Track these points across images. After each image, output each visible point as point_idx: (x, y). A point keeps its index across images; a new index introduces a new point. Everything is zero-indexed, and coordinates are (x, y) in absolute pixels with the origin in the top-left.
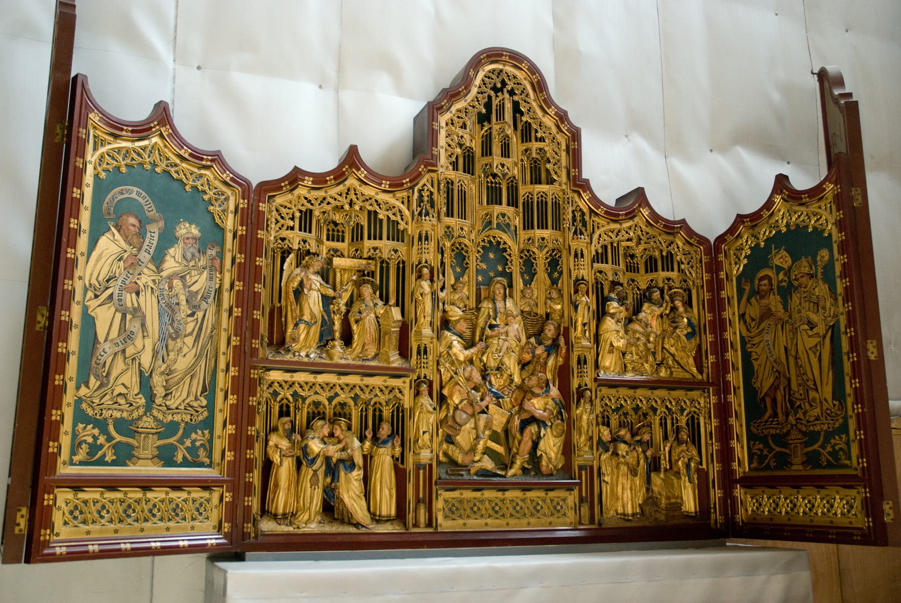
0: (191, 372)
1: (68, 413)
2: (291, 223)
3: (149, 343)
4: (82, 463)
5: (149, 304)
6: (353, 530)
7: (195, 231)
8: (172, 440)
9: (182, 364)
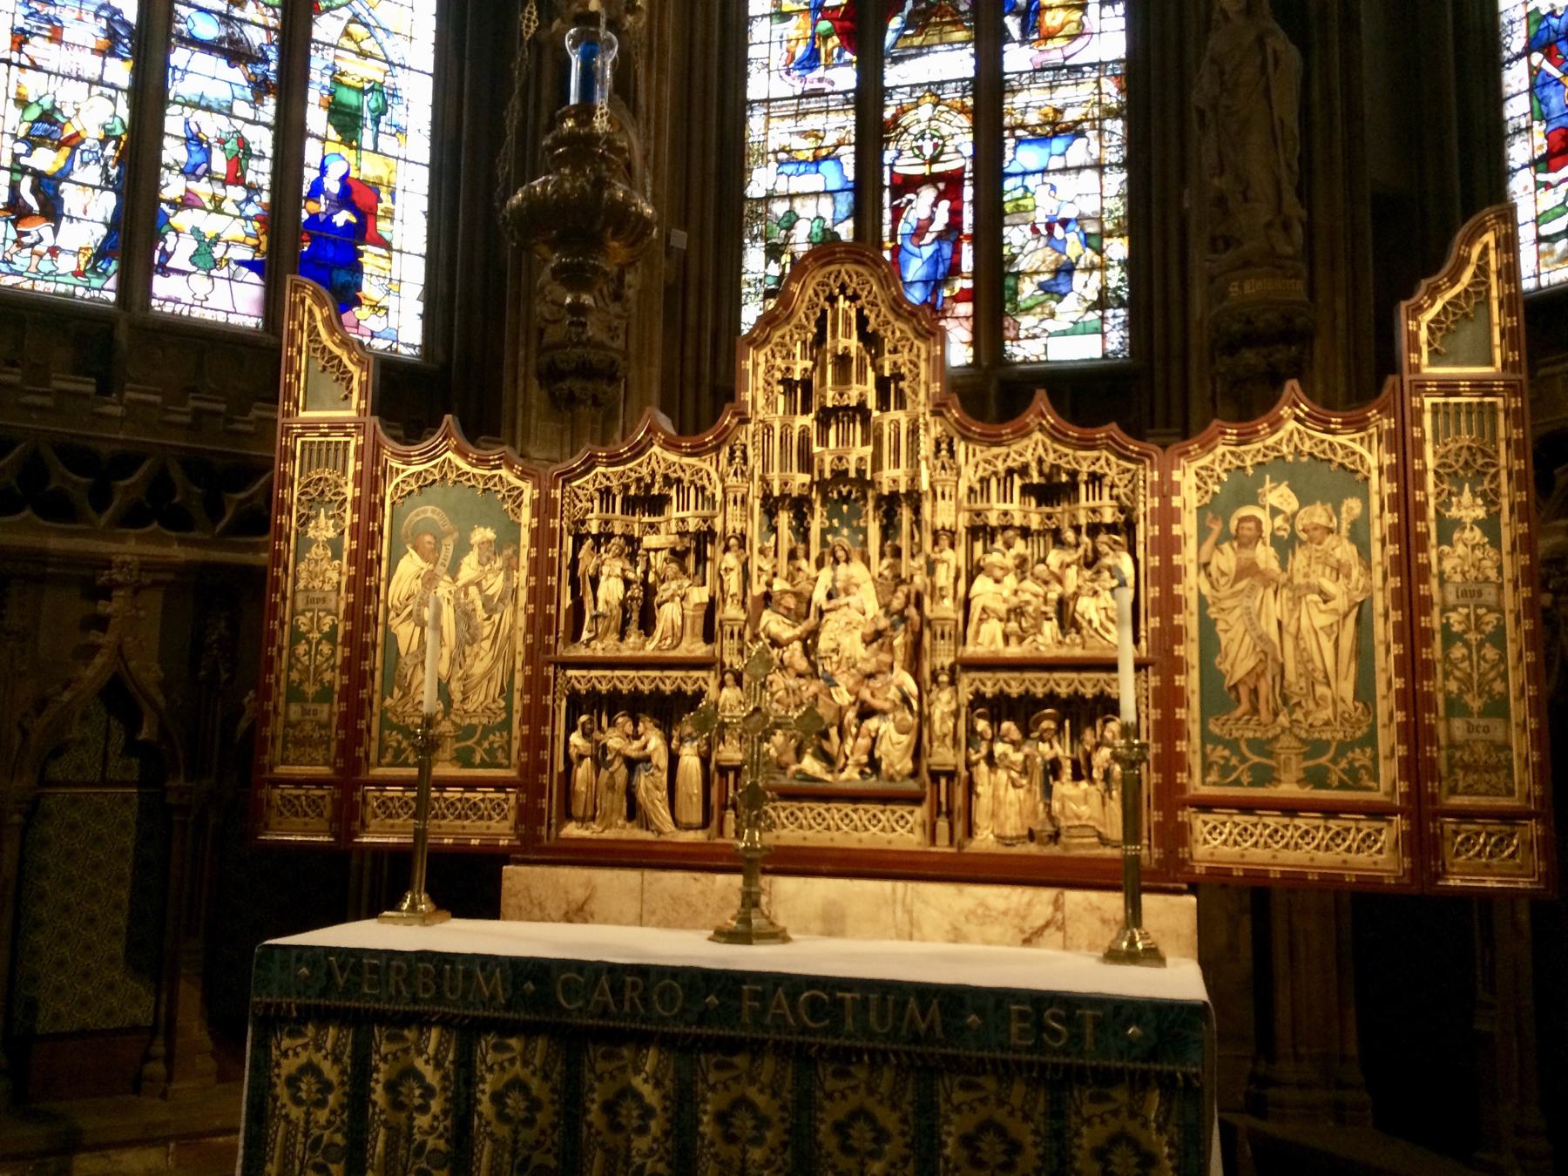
0: (488, 675)
2: (589, 505)
7: (490, 534)
8: (470, 743)
9: (479, 669)
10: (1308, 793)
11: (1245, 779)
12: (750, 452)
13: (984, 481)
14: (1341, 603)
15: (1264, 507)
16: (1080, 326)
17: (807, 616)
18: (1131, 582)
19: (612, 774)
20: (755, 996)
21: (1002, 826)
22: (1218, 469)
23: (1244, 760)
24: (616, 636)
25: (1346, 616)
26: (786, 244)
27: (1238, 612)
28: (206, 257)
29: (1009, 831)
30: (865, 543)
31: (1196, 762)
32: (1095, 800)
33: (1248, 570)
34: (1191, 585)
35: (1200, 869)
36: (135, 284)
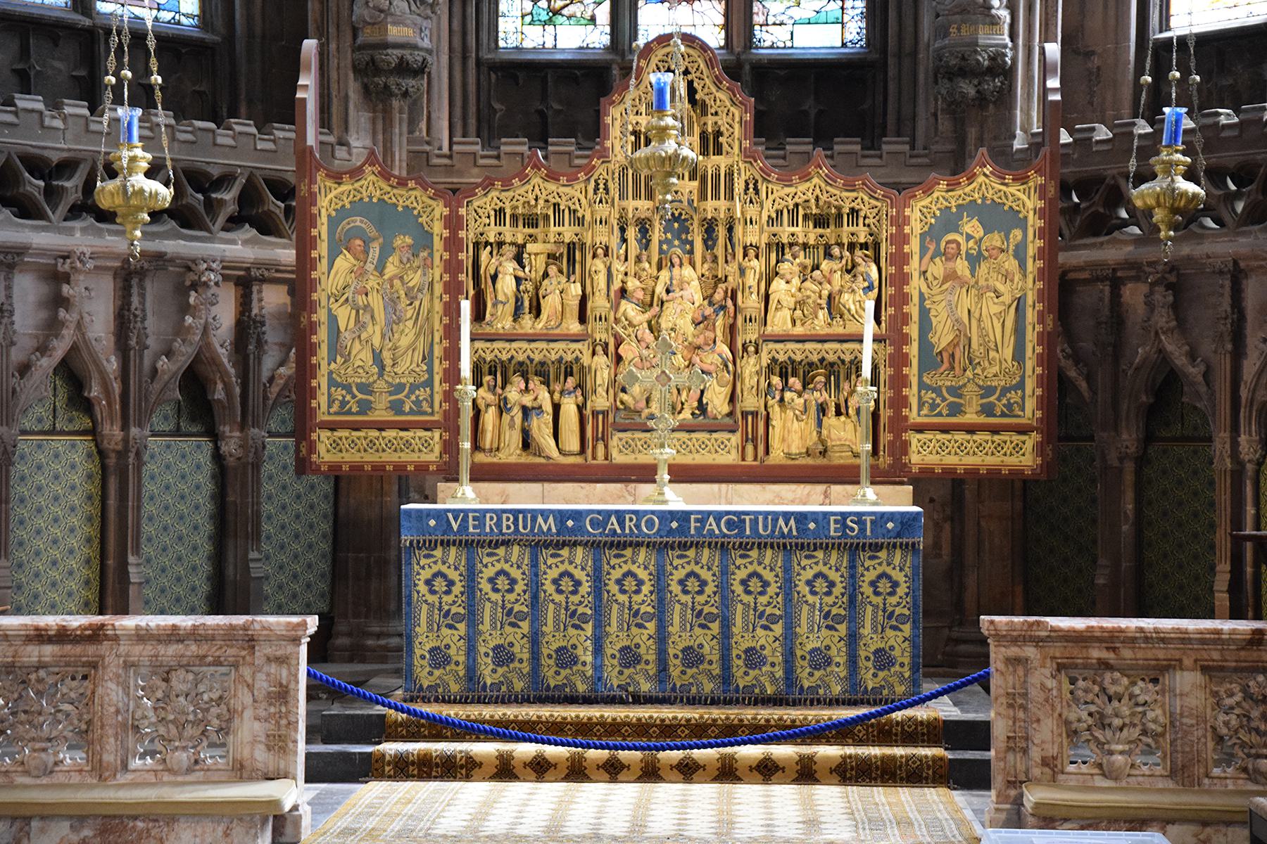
1: (324, 382)
2: (488, 221)
3: (377, 329)
4: (336, 413)
5: (376, 301)
6: (542, 460)
7: (409, 240)
8: (400, 396)
9: (404, 342)
10: (983, 419)
11: (945, 412)
12: (610, 184)
13: (779, 213)
14: (1007, 298)
15: (962, 234)
16: (823, 15)
17: (651, 305)
18: (876, 284)
19: (512, 417)
20: (697, 520)
21: (789, 447)
22: (934, 208)
23: (944, 399)
24: (511, 319)
25: (1010, 306)
27: (944, 303)
29: (794, 450)
30: (691, 252)
31: (914, 402)
32: (850, 427)
33: (951, 276)
34: (915, 286)
35: (915, 470)
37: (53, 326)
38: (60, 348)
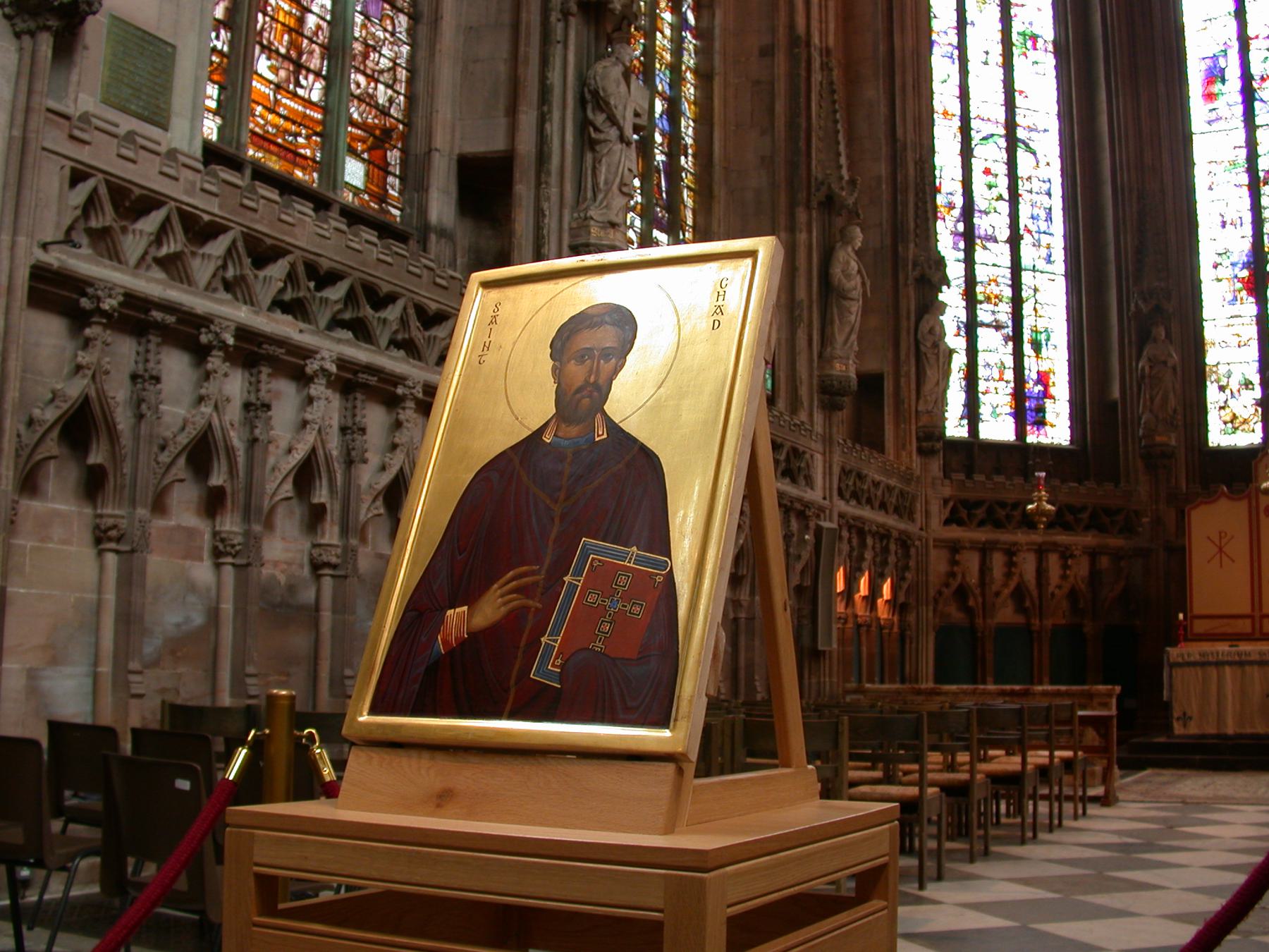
26: (1228, 385)
28: (995, 414)
36: (973, 429)
37: (1008, 575)
38: (1013, 584)
